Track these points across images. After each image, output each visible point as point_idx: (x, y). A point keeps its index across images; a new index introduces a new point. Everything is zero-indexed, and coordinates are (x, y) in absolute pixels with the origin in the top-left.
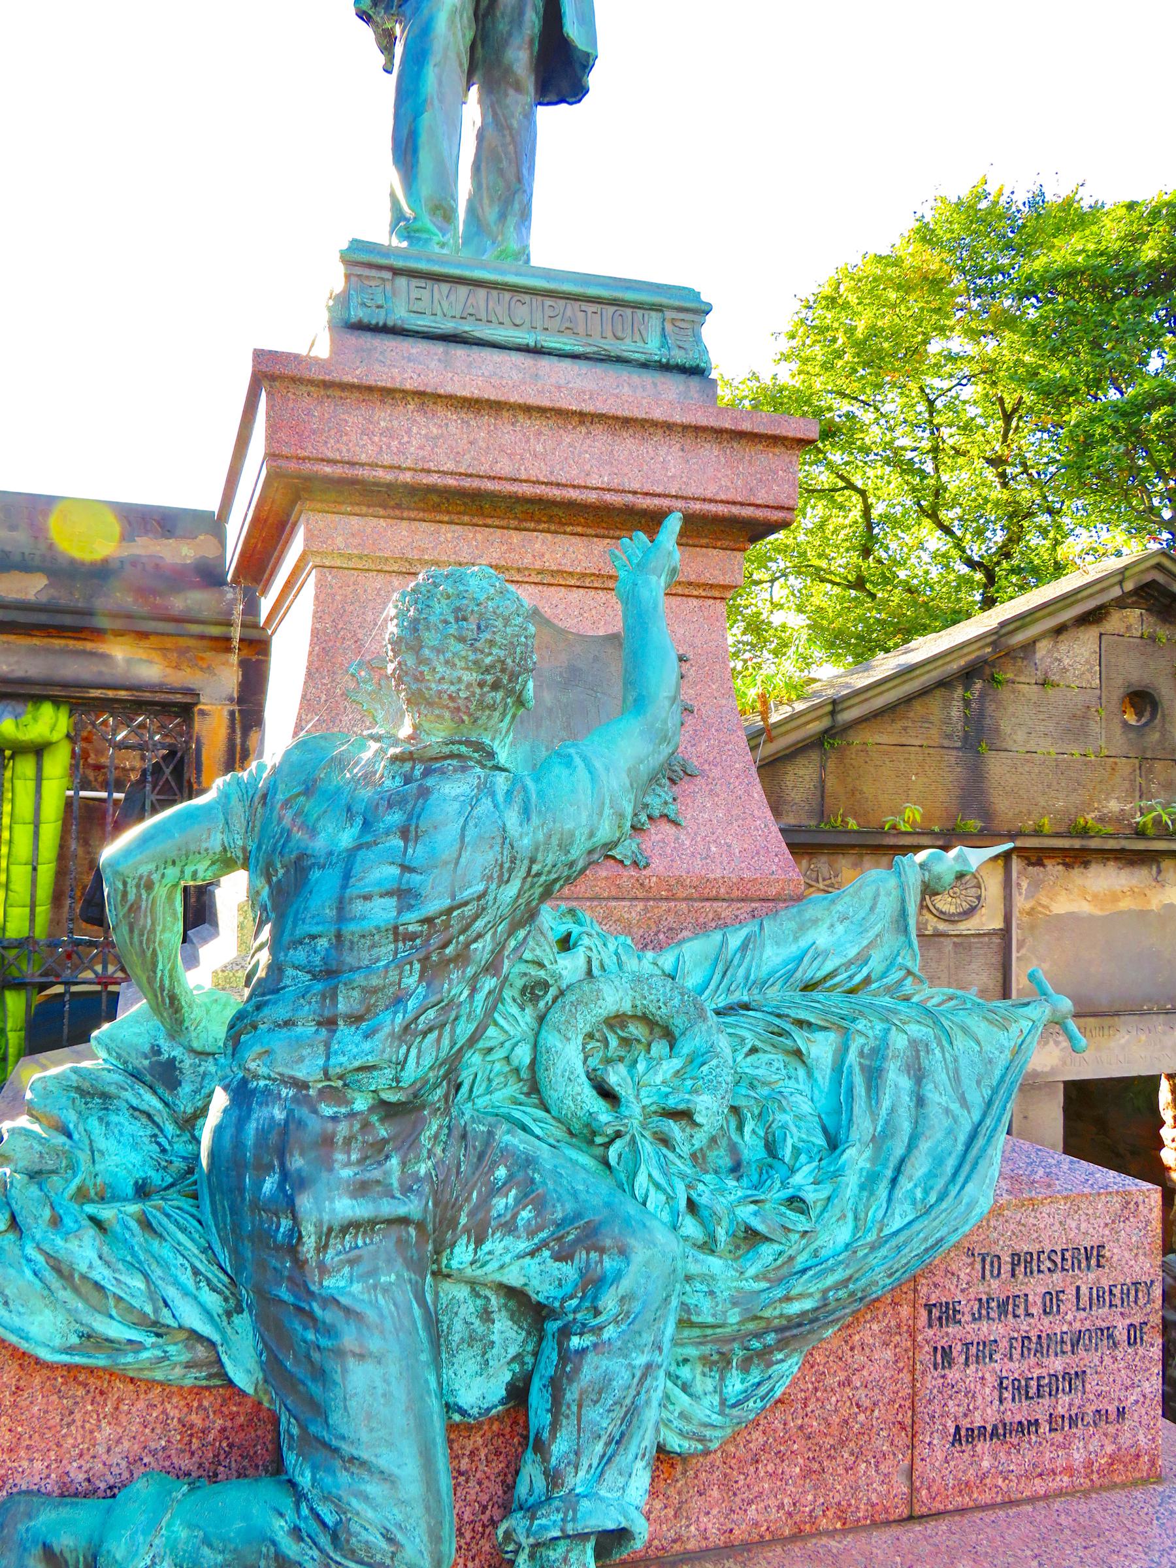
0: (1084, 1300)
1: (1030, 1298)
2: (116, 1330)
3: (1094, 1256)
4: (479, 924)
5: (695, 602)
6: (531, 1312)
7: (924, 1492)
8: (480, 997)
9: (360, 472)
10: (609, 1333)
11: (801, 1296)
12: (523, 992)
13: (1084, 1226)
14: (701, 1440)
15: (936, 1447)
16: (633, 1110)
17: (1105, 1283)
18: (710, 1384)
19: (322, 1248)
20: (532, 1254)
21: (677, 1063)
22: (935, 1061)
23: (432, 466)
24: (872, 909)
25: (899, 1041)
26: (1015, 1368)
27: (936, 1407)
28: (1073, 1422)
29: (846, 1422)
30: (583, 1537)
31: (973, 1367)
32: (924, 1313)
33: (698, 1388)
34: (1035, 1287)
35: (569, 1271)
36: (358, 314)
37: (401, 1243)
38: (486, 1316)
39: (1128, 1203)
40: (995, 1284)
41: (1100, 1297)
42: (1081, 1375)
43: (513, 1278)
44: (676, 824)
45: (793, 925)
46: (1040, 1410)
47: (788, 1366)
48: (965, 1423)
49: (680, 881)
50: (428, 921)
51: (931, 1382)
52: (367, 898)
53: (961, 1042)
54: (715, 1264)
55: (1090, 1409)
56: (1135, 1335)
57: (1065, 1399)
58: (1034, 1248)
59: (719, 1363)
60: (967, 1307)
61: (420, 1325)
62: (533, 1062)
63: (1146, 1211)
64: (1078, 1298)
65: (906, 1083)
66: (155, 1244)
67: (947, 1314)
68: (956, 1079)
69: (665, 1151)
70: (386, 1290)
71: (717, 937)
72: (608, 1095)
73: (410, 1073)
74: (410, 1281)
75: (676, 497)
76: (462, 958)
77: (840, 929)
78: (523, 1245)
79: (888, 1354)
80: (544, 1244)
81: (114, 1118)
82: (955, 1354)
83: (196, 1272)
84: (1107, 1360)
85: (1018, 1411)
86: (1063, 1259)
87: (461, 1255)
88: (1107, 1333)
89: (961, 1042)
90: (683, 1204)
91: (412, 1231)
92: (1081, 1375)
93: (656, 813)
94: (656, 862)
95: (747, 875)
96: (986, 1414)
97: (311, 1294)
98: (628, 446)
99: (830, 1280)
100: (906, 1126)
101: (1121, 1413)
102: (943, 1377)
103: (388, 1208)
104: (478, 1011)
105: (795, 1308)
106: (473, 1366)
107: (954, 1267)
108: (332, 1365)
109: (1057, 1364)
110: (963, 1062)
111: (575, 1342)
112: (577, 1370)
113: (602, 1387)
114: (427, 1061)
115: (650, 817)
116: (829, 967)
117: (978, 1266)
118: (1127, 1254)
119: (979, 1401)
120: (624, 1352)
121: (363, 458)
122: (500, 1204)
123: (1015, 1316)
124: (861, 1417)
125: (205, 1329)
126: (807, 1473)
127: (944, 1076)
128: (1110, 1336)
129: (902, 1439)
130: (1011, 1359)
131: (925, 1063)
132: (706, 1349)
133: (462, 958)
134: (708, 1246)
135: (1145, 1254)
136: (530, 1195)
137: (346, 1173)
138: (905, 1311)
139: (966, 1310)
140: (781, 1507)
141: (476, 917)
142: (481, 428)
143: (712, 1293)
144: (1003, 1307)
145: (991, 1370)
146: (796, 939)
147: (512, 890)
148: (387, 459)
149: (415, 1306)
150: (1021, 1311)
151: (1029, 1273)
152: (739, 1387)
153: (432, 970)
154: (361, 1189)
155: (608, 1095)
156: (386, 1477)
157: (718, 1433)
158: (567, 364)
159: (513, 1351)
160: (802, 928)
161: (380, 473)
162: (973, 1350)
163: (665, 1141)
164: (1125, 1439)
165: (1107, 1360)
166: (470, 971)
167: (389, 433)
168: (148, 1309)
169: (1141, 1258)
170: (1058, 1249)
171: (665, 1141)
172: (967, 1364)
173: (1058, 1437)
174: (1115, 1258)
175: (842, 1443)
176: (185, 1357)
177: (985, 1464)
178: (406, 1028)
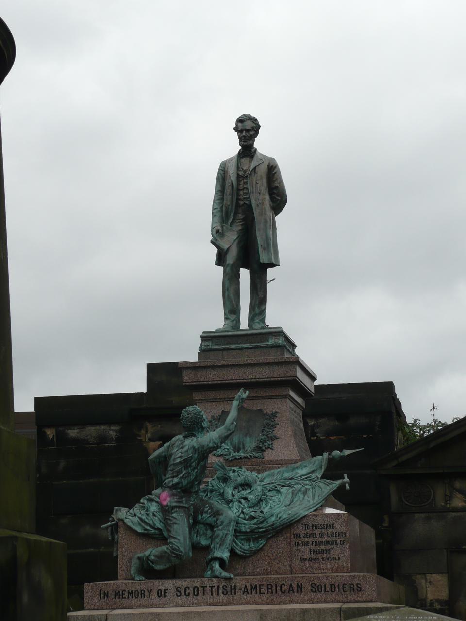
0: (329, 535)
2: (148, 528)
3: (332, 526)
4: (192, 461)
5: (280, 400)
6: (211, 527)
7: (294, 570)
8: (194, 472)
9: (201, 383)
10: (220, 528)
12: (223, 480)
14: (245, 553)
15: (296, 562)
16: (236, 497)
18: (247, 545)
19: (172, 510)
20: (210, 516)
21: (250, 491)
22: (310, 493)
23: (214, 380)
24: (313, 465)
25: (303, 489)
26: (313, 548)
27: (296, 553)
28: (328, 559)
30: (216, 559)
32: (293, 535)
33: (245, 545)
34: (318, 532)
35: (215, 519)
36: (204, 347)
37: (185, 511)
38: (206, 530)
40: (308, 530)
41: (333, 535)
42: (329, 550)
43: (208, 521)
44: (272, 449)
46: (320, 556)
47: (262, 542)
48: (303, 557)
49: (271, 461)
50: (184, 460)
51: (294, 549)
52: (177, 458)
53: (317, 489)
54: (245, 521)
55: (332, 557)
56: (342, 543)
59: (248, 540)
60: (302, 535)
62: (223, 492)
65: (302, 496)
66: (155, 517)
67: (298, 536)
68: (314, 496)
69: (240, 504)
70: (181, 516)
71: (273, 471)
72: (233, 496)
73: (184, 484)
75: (268, 378)
76: (190, 466)
77: (304, 469)
78: (209, 515)
79: (285, 542)
80: (212, 515)
81: (153, 503)
83: (160, 521)
84: (335, 547)
85: (314, 556)
86: (324, 527)
87: (200, 518)
88: (336, 542)
89: (317, 489)
90: (240, 512)
91: (187, 510)
92: (329, 550)
94: (266, 458)
95: (286, 459)
96: (307, 556)
97: (170, 516)
98: (257, 369)
99: (267, 525)
100: (298, 503)
101: (339, 559)
103: (181, 505)
105: (261, 530)
106: (204, 538)
108: (172, 525)
109: (323, 547)
110: (317, 492)
111: (215, 529)
112: (215, 533)
113: (218, 536)
114: (187, 481)
115: (266, 448)
116: (297, 476)
117: (304, 527)
119: (306, 553)
120: (221, 530)
121: (201, 380)
122: (206, 510)
124: (280, 554)
125: (160, 527)
126: (269, 564)
129: (289, 559)
130: (312, 545)
131: (308, 492)
132: (245, 537)
133: (190, 466)
134: (245, 519)
136: (211, 508)
138: (288, 535)
140: (264, 569)
141: (192, 459)
142: (225, 371)
143: (245, 527)
144: (310, 535)
145: (307, 547)
146: (292, 471)
147: (196, 455)
148: (206, 380)
150: (314, 536)
151: (316, 529)
152: (253, 545)
153: (186, 468)
154: (176, 502)
155: (233, 496)
156: (178, 539)
157: (247, 552)
158: (249, 350)
159: (210, 535)
160: (294, 469)
161: (205, 383)
162: (304, 543)
163: (240, 502)
164: (341, 564)
165: (335, 547)
166: (192, 468)
167: (206, 374)
168: (153, 525)
171: (240, 502)
172: (302, 546)
173: (324, 562)
175: (276, 559)
176: (158, 533)
177: (307, 566)
178: (182, 477)
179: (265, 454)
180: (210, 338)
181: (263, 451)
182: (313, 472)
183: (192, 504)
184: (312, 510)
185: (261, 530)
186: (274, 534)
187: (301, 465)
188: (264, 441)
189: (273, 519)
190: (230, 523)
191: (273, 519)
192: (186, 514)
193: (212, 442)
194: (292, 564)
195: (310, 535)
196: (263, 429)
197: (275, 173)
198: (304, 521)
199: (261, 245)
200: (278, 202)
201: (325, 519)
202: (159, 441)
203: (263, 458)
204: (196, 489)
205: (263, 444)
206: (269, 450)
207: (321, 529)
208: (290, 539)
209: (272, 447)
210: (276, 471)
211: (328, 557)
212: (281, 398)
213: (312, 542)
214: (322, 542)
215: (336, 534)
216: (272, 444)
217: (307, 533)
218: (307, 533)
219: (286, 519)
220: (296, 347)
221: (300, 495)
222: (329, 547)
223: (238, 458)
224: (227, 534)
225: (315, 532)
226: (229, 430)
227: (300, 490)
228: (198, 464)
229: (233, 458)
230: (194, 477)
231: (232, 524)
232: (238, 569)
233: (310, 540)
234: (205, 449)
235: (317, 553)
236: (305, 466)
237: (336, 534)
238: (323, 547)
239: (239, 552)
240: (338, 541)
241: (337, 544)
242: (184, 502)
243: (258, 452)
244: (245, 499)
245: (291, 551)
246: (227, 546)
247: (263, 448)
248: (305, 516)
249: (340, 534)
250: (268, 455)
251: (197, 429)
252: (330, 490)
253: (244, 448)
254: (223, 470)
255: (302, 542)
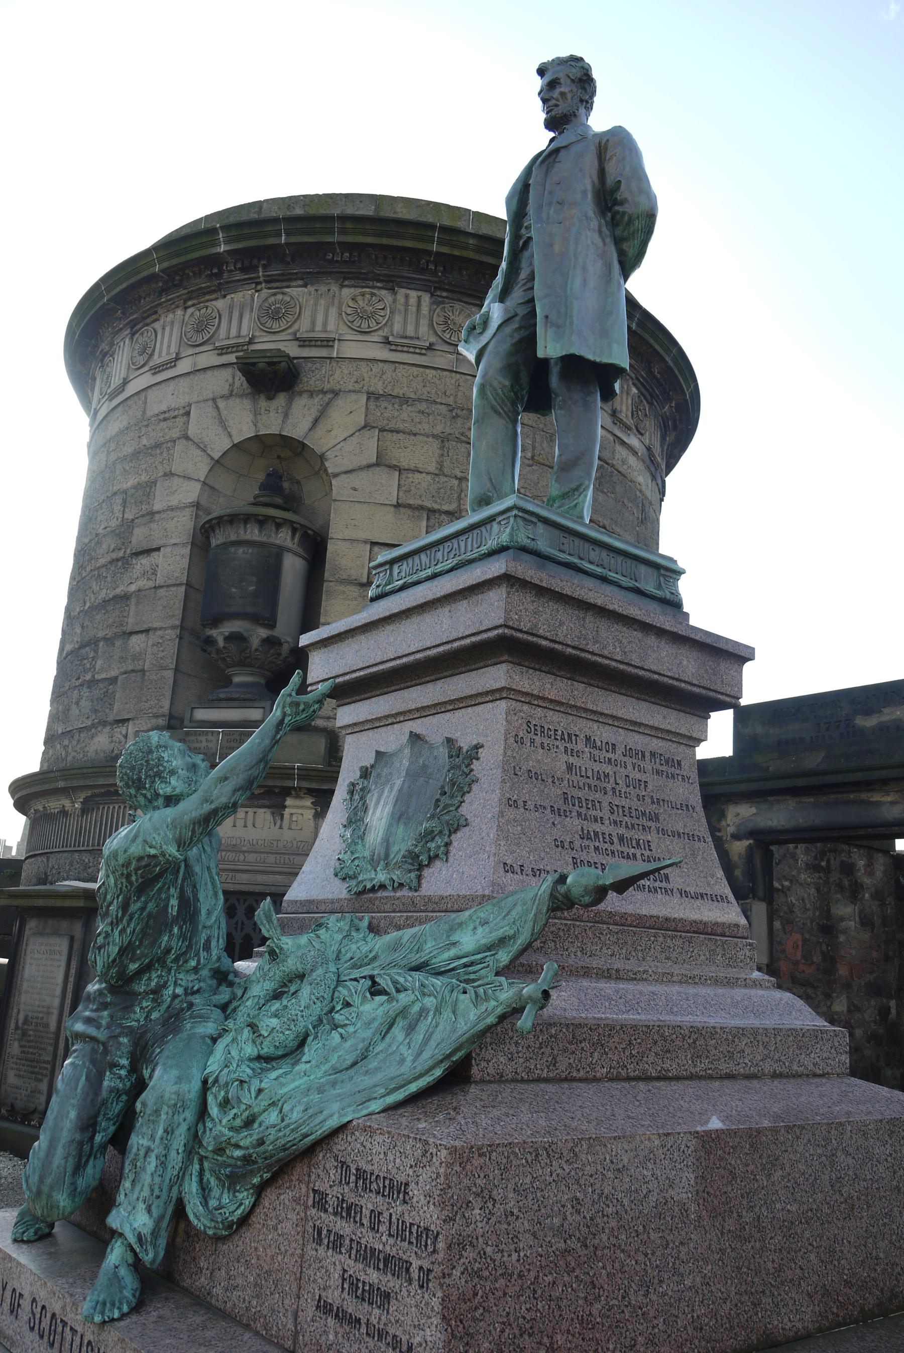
1: (364, 1210)
4: (109, 897)
11: (237, 1146)
13: (398, 1161)
17: (408, 1220)
25: (416, 1008)
29: (273, 1256)
31: (331, 1251)
32: (312, 1195)
34: (369, 1202)
37: (94, 1051)
39: (426, 1152)
41: (401, 1231)
45: (446, 927)
57: (376, 1311)
58: (369, 1168)
60: (332, 1201)
61: (80, 1087)
63: (437, 1164)
64: (390, 1224)
74: (88, 1068)
77: (480, 930)
82: (323, 1236)
85: (351, 1306)
86: (384, 1187)
92: (387, 1296)
93: (432, 854)
95: (463, 892)
102: (316, 1250)
103: (92, 1031)
104: (117, 941)
107: (327, 1166)
109: (373, 1276)
110: (440, 1027)
117: (339, 1171)
118: (422, 1198)
123: (355, 1222)
127: (422, 1036)
128: (408, 1270)
130: (350, 1257)
135: (434, 1204)
137: (87, 1013)
139: (331, 1203)
140: (244, 1300)
141: (106, 894)
147: (112, 880)
149: (84, 1078)
154: (88, 1021)
160: (452, 930)
166: (109, 920)
169: (432, 1207)
170: (382, 1175)
174: (415, 1200)
177: (331, 1337)
179: (426, 872)
180: (387, 567)
181: (421, 867)
182: (502, 941)
183: (130, 1031)
184: (375, 1106)
185: (238, 1153)
186: (266, 1176)
187: (471, 917)
188: (429, 835)
189: (273, 1117)
190: (157, 1112)
191: (273, 1117)
192: (93, 1061)
193: (140, 840)
194: (300, 1313)
195: (349, 1209)
196: (438, 796)
197: (614, 155)
198: (340, 1145)
199: (547, 317)
200: (626, 218)
201: (389, 1154)
202: (748, 839)
203: (416, 891)
204: (153, 984)
205: (427, 842)
206: (438, 864)
207: (378, 1193)
208: (306, 1207)
209: (447, 853)
210: (407, 934)
211: (381, 1327)
212: (492, 701)
213: (352, 1240)
214: (373, 1250)
215: (411, 1232)
216: (447, 845)
217: (343, 1200)
218: (343, 1200)
219: (287, 1131)
220: (679, 573)
221: (398, 1032)
222: (389, 1282)
223: (369, 886)
224: (149, 1150)
225: (363, 1202)
226: (207, 801)
227: (403, 1012)
228: (125, 907)
229: (360, 888)
230: (116, 949)
231: (163, 1117)
232: (201, 1272)
233: (344, 1227)
234: (121, 860)
235: (357, 1297)
236: (485, 923)
237: (411, 1232)
238: (373, 1276)
239: (191, 1217)
240: (416, 1263)
241: (410, 1281)
242: (104, 1022)
243: (410, 871)
244: (253, 1027)
245: (302, 1256)
246: (146, 1192)
247: (424, 858)
248: (342, 1128)
249: (424, 1236)
250: (438, 881)
251: (142, 800)
252: (480, 1019)
253: (387, 855)
254: (267, 926)
255: (329, 1231)
